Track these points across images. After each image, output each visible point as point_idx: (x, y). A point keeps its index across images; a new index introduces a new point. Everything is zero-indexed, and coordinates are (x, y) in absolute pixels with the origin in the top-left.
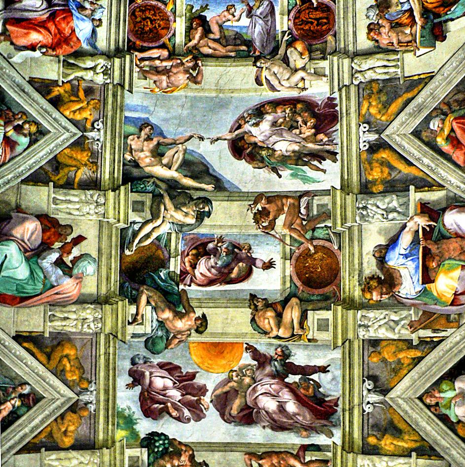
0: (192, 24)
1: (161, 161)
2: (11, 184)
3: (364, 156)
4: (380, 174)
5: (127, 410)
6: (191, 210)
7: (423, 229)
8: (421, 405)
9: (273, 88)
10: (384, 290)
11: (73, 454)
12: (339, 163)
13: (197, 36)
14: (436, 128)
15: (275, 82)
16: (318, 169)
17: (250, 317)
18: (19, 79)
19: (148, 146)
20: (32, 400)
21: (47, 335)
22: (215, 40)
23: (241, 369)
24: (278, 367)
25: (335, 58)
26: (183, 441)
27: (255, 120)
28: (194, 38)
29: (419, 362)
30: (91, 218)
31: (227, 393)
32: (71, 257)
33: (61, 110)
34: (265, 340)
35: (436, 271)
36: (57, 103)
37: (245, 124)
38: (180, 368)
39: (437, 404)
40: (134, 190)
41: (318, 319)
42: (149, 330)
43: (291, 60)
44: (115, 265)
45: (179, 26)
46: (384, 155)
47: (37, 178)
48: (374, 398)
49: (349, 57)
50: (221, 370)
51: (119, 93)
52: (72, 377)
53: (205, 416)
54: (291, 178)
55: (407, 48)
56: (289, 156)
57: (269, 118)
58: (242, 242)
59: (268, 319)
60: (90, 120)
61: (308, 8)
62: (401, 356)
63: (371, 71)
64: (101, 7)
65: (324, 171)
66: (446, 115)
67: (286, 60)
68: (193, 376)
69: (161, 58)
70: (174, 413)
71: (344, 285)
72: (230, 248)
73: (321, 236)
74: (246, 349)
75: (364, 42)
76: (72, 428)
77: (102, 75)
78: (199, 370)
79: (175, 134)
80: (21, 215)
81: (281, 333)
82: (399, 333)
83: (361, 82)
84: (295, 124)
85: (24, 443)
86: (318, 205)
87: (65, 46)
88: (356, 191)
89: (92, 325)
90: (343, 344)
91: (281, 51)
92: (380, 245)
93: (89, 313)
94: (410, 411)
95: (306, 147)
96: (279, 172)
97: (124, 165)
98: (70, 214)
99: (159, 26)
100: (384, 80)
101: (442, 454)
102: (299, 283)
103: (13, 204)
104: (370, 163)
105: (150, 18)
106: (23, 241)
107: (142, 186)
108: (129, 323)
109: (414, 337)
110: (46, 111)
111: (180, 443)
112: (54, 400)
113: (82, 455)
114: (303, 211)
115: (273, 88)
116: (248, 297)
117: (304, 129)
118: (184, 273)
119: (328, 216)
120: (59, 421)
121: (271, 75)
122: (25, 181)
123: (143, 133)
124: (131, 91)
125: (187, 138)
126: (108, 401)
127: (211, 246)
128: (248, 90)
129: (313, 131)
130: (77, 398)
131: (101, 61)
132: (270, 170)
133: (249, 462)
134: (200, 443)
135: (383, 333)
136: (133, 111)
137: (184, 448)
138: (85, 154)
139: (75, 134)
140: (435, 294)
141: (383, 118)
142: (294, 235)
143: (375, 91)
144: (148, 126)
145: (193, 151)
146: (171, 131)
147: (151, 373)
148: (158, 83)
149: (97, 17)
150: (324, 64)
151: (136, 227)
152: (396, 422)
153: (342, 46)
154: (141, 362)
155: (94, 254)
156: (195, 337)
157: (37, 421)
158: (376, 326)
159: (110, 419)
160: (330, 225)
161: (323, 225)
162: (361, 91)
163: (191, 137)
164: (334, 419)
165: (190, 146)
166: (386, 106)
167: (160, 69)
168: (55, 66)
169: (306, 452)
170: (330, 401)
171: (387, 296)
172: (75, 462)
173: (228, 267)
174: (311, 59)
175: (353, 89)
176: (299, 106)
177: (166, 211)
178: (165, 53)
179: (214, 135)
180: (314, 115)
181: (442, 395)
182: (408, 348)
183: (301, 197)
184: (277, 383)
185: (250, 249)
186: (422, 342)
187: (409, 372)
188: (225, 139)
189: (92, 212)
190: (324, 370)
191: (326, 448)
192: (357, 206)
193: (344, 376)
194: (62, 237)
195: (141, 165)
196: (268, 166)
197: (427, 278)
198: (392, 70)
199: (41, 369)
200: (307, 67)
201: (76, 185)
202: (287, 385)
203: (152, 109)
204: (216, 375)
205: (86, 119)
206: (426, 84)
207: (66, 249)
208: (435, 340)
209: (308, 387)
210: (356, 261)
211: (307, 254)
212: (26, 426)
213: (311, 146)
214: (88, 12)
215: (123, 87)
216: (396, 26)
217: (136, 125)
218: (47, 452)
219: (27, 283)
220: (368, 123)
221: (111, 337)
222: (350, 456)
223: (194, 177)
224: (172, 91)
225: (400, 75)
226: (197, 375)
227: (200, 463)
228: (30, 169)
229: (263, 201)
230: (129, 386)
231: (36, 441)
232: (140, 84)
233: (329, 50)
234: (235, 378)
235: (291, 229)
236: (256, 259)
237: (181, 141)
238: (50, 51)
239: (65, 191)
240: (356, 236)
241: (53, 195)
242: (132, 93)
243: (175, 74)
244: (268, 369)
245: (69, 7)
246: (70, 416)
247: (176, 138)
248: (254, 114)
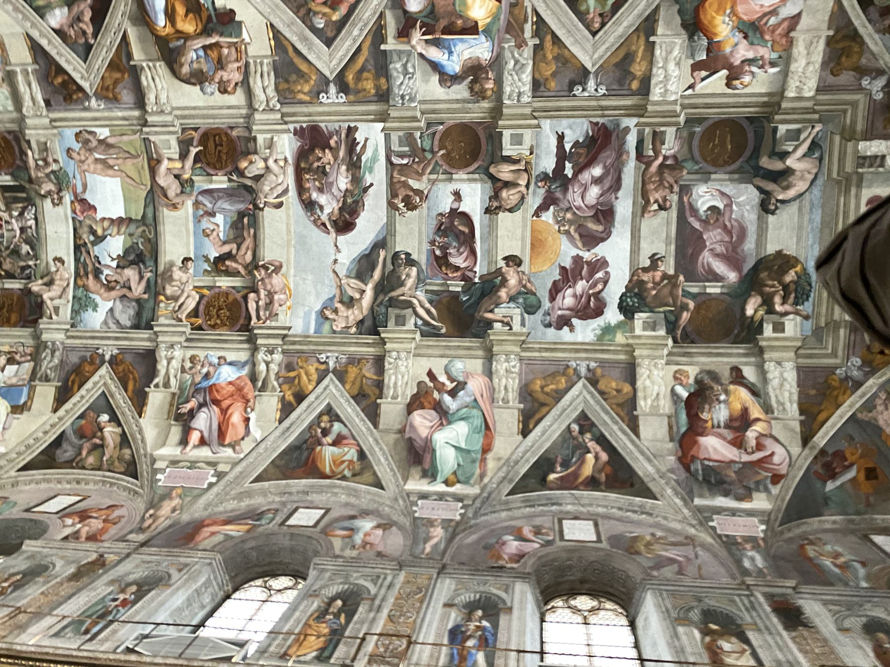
0: (223, 271)
1: (356, 300)
2: (378, 437)
3: (352, 98)
4: (370, 81)
5: (596, 332)
6: (404, 272)
7: (424, 34)
8: (601, 33)
9: (286, 191)
10: (483, 76)
11: (639, 384)
12: (358, 124)
13: (234, 265)
14: (323, 21)
15: (280, 189)
16: (364, 146)
17: (507, 214)
18: (278, 433)
20: (585, 422)
21: (522, 406)
22: (238, 249)
23: (558, 222)
24: (557, 185)
25: (255, 128)
26: (628, 278)
28: (236, 269)
29: (557, 37)
30: (410, 364)
31: (581, 236)
32: (448, 383)
33: (307, 392)
34: (529, 199)
35: (466, 19)
36: (300, 397)
38: (555, 282)
39: (601, 15)
41: (511, 144)
42: (518, 311)
43: (257, 173)
44: (455, 342)
45: (224, 282)
46: (350, 77)
47: (373, 414)
48: (591, 84)
49: (253, 114)
50: (558, 241)
51: (292, 339)
52: (563, 383)
53: (603, 258)
55: (243, 52)
56: (352, 175)
57: (315, 195)
58: (435, 222)
59: (509, 196)
61: (205, 155)
62: (550, 56)
63: (267, 90)
64: (206, 357)
65: (366, 140)
66: (310, 10)
67: (257, 178)
68: (563, 269)
70: (600, 287)
71: (478, 118)
72: (440, 233)
73: (430, 142)
74: (538, 217)
75: (238, 98)
76: (614, 385)
78: (557, 263)
80: (407, 429)
81: (523, 182)
82: (527, 59)
83: (278, 101)
84: (320, 169)
85: (628, 431)
86: (400, 146)
87: (245, 390)
88: (386, 107)
89: (512, 364)
90: (536, 118)
91: (249, 183)
92: (440, 81)
93: (500, 366)
94: (607, 45)
96: (368, 185)
97: (361, 334)
98: (407, 383)
99: (225, 301)
100: (276, 77)
101: (653, 7)
102: (475, 165)
103: (398, 436)
104: (359, 92)
105: (217, 311)
106: (432, 427)
108: (511, 329)
109: (532, 42)
110: (308, 407)
111: (630, 281)
112: (586, 401)
113: (641, 376)
114: (405, 161)
115: (286, 191)
116: (488, 215)
117: (325, 160)
118: (464, 278)
120: (605, 397)
121: (272, 193)
122: (376, 425)
123: (330, 316)
124: (289, 328)
126: (586, 351)
127: (438, 252)
128: (288, 216)
129: (327, 151)
130: (583, 380)
131: (261, 356)
133: (652, 213)
134: (631, 262)
135: (527, 77)
137: (636, 278)
138: (350, 370)
139: (331, 379)
140: (489, 20)
141: (314, 78)
142: (428, 171)
143: (286, 86)
146: (329, 290)
147: (560, 309)
149: (216, 361)
150: (261, 138)
151: (420, 322)
152: (616, 60)
153: (242, 120)
154: (548, 318)
155: (445, 361)
156: (525, 268)
157: (606, 418)
158: (520, 84)
159: (605, 348)
160: (418, 134)
161: (419, 141)
162: (287, 101)
163: (335, 272)
164: (610, 126)
165: (342, 273)
166: (301, 75)
167: (268, 301)
169: (645, 154)
170: (593, 131)
171: (490, 73)
172: (648, 383)
173: (458, 235)
174: (256, 152)
175: (286, 110)
176: (303, 165)
178: (252, 296)
179: (332, 249)
180: (312, 150)
181: (592, 10)
182: (542, 49)
183: (392, 164)
184: (573, 186)
185: (441, 214)
186: (536, 34)
187: (566, 47)
189: (405, 364)
190: (561, 138)
191: (641, 135)
193: (568, 117)
194: (429, 390)
197: (472, 29)
198: (265, 69)
199: (555, 412)
200: (263, 156)
201: (381, 378)
202: (576, 175)
203: (307, 309)
204: (562, 247)
205: (317, 369)
206: (278, 31)
207: (440, 387)
208: (535, 19)
209: (578, 153)
210: (455, 106)
211: (447, 158)
212: (612, 429)
213: (342, 154)
214: (211, 369)
215: (285, 336)
216: (221, 64)
217: (322, 324)
218: (638, 408)
219: (472, 424)
220: (319, 94)
221: (524, 346)
222: (650, 108)
223: (373, 269)
224: (290, 290)
225: (270, 60)
226: (562, 265)
227: (651, 262)
228: (364, 421)
229: (396, 201)
230: (572, 328)
231: (626, 419)
232: (283, 319)
233: (247, 134)
234: (567, 228)
235: (422, 175)
236: (451, 209)
238: (250, 404)
239: (385, 389)
240: (430, 107)
241: (389, 399)
244: (559, 195)
246: (602, 385)
247: (335, 286)
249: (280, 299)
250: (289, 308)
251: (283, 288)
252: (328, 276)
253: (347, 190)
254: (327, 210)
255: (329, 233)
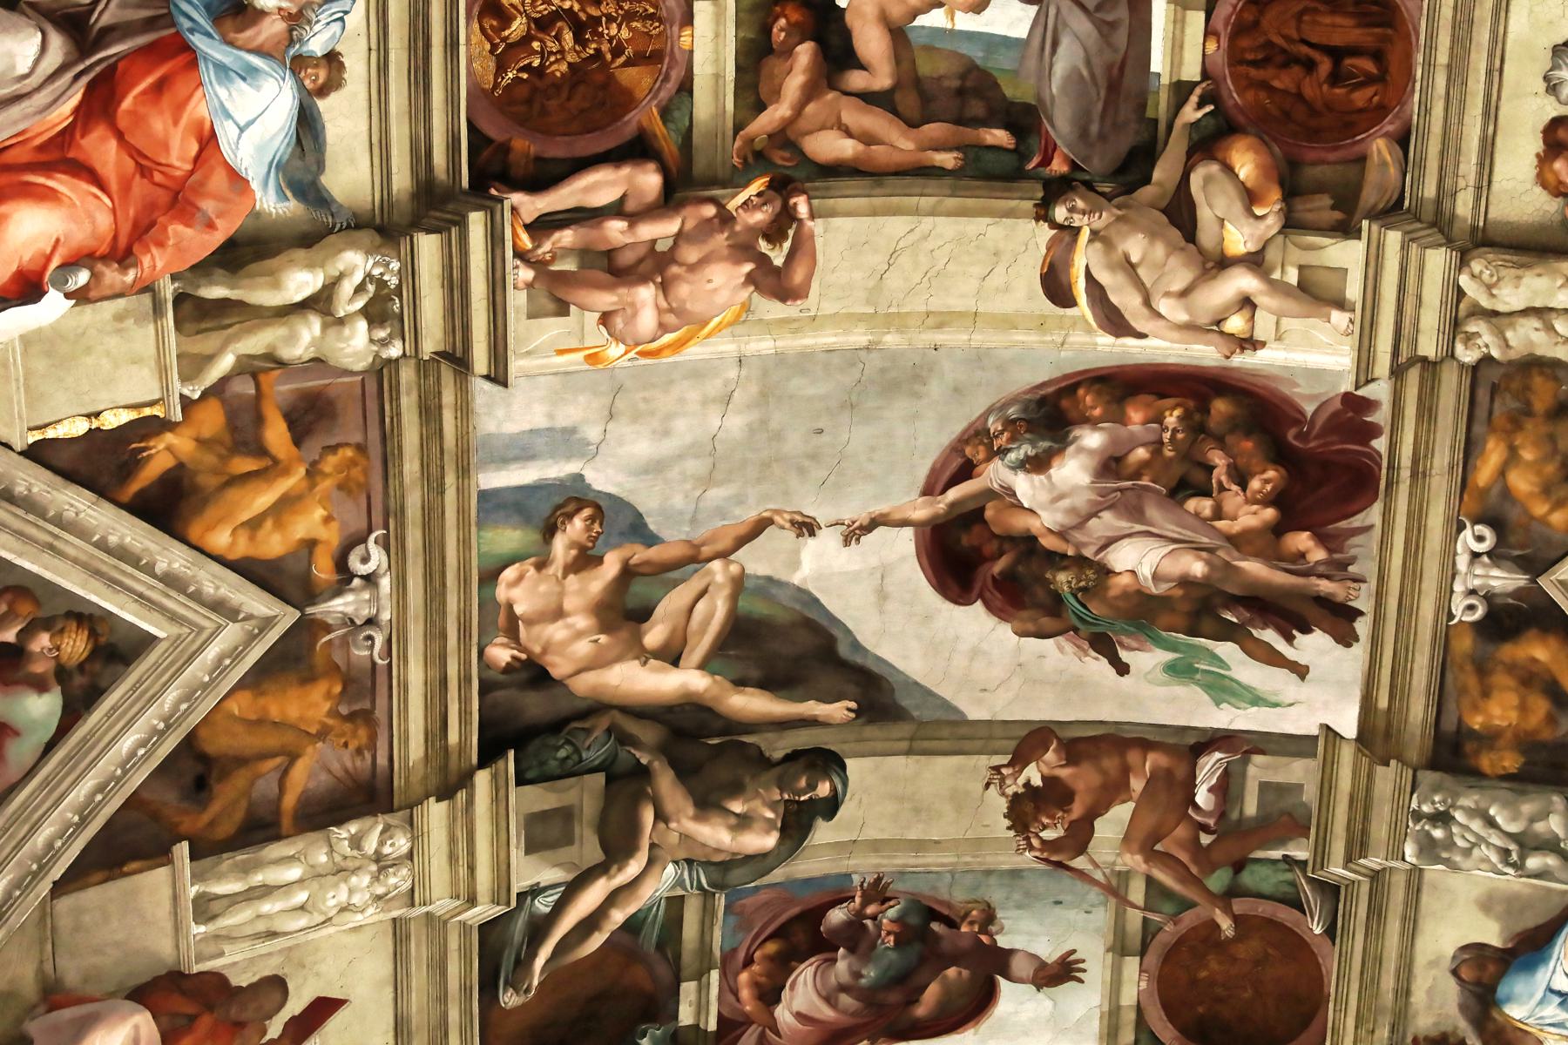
1: (637, 639)
13: (794, 83)
16: (1273, 658)
19: (580, 592)
27: (1033, 444)
37: (989, 459)
40: (530, 775)
54: (1165, 677)
56: (1163, 601)
57: (1092, 439)
60: (327, 542)
65: (1301, 671)
69: (631, 206)
77: (362, 325)
79: (694, 521)
86: (1264, 787)
95: (1237, 568)
96: (1124, 655)
97: (485, 688)
99: (617, 51)
107: (562, 753)
114: (1203, 797)
119: (1295, 825)
124: (498, 377)
125: (742, 530)
132: (1086, 645)
136: (516, 459)
144: (578, 510)
145: (769, 579)
148: (619, 322)
149: (316, 45)
160: (1301, 854)
163: (760, 527)
167: (627, 258)
168: (143, 338)
177: (662, 826)
179: (856, 509)
188: (904, 523)
192: (1414, 805)
195: (556, 673)
196: (1076, 630)
203: (593, 433)
214: (272, 28)
215: (458, 359)
223: (772, 683)
237: (721, 546)
242: (505, 384)
243: (692, 268)
245: (173, 24)
247: (699, 534)
248: (1028, 421)
249: (633, 311)
250: (593, 359)
251: (679, 312)
252: (740, 500)
253: (1106, 572)
254: (1025, 486)
255: (928, 491)
